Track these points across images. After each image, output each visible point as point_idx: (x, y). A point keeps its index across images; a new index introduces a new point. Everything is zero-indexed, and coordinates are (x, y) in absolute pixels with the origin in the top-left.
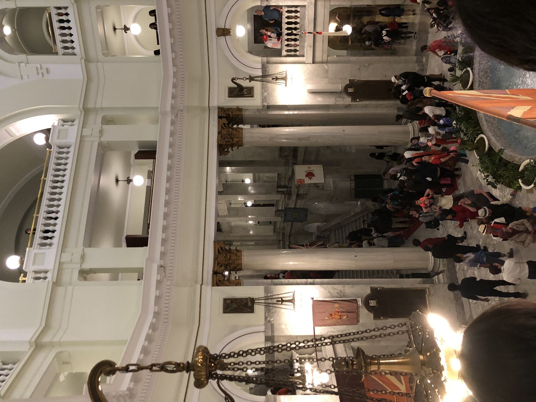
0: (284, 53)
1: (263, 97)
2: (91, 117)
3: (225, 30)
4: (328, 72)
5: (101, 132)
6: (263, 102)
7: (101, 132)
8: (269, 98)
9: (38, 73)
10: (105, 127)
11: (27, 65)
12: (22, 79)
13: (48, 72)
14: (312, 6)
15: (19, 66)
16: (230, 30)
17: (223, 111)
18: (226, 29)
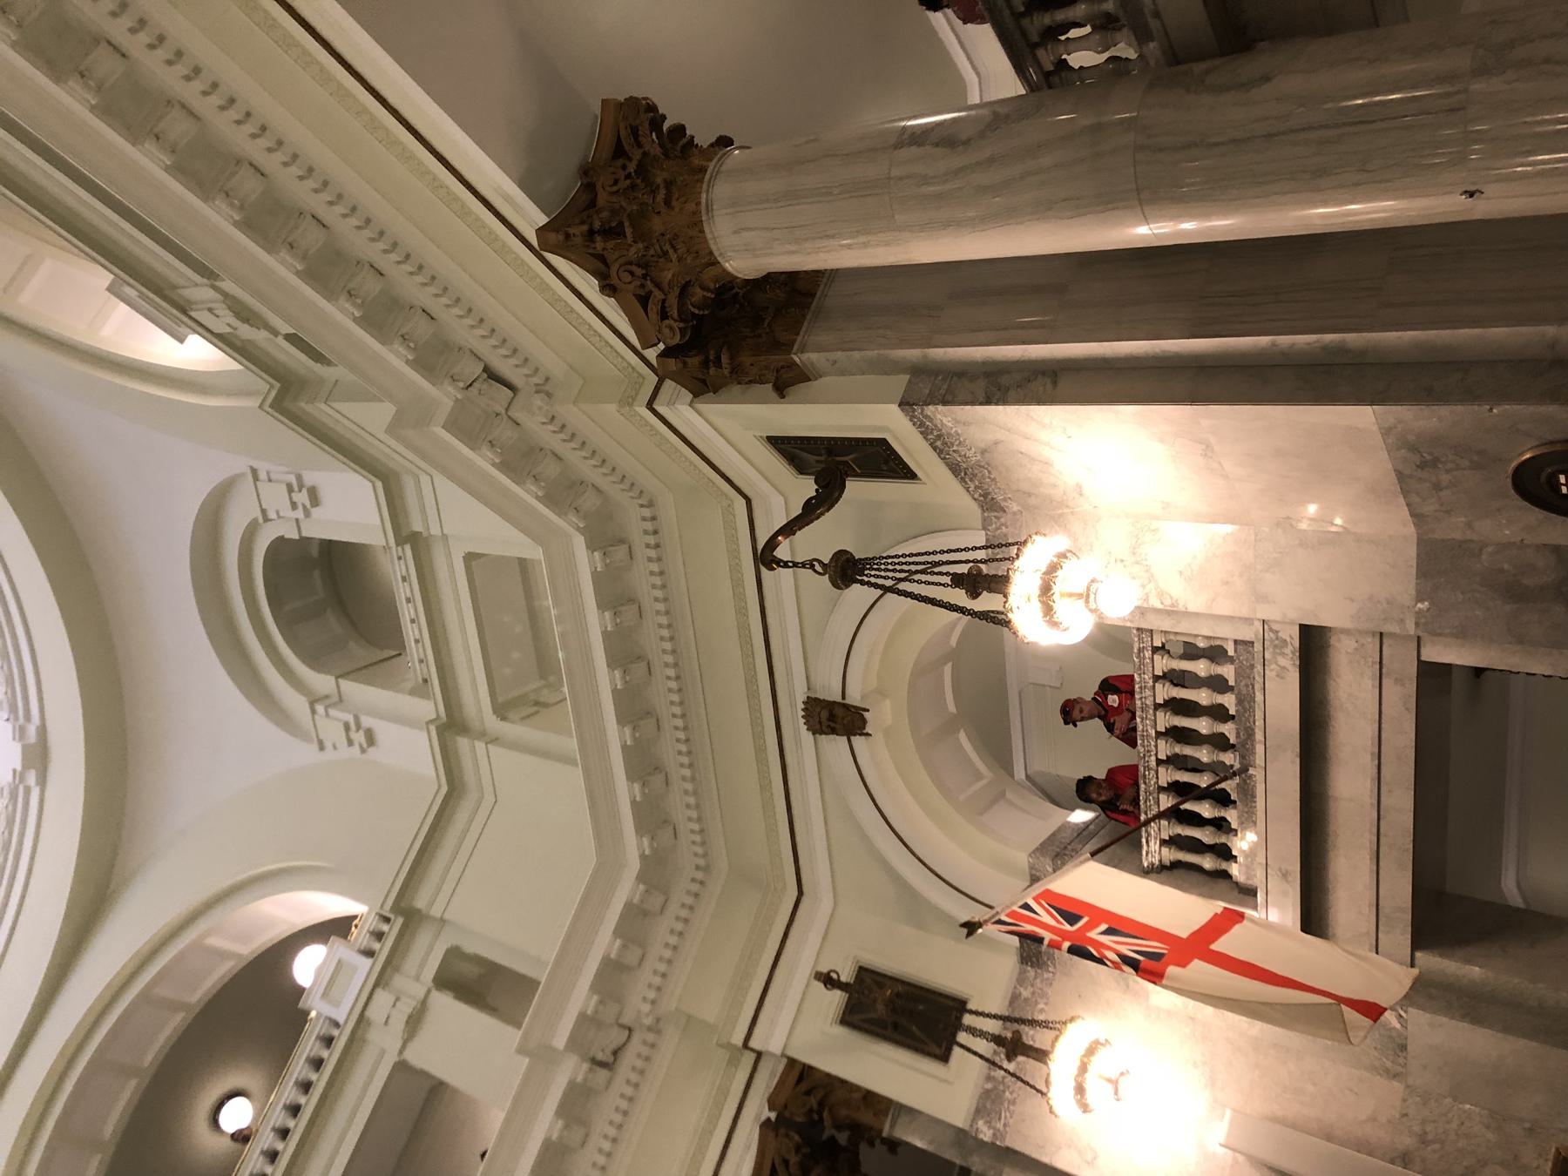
0: (1153, 851)
1: (989, 1086)
2: (422, 939)
3: (839, 712)
4: (1403, 1048)
5: (414, 1022)
6: (979, 1112)
7: (414, 1022)
8: (1013, 1102)
9: (350, 743)
10: (444, 1002)
11: (332, 712)
12: (322, 747)
13: (371, 738)
14: (1282, 661)
15: (314, 712)
16: (866, 714)
17: (804, 1086)
18: (847, 707)
